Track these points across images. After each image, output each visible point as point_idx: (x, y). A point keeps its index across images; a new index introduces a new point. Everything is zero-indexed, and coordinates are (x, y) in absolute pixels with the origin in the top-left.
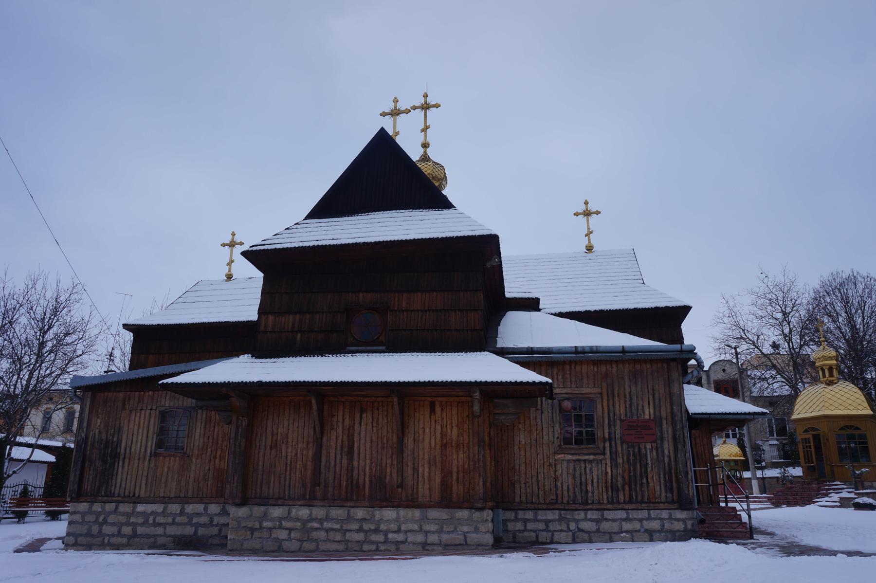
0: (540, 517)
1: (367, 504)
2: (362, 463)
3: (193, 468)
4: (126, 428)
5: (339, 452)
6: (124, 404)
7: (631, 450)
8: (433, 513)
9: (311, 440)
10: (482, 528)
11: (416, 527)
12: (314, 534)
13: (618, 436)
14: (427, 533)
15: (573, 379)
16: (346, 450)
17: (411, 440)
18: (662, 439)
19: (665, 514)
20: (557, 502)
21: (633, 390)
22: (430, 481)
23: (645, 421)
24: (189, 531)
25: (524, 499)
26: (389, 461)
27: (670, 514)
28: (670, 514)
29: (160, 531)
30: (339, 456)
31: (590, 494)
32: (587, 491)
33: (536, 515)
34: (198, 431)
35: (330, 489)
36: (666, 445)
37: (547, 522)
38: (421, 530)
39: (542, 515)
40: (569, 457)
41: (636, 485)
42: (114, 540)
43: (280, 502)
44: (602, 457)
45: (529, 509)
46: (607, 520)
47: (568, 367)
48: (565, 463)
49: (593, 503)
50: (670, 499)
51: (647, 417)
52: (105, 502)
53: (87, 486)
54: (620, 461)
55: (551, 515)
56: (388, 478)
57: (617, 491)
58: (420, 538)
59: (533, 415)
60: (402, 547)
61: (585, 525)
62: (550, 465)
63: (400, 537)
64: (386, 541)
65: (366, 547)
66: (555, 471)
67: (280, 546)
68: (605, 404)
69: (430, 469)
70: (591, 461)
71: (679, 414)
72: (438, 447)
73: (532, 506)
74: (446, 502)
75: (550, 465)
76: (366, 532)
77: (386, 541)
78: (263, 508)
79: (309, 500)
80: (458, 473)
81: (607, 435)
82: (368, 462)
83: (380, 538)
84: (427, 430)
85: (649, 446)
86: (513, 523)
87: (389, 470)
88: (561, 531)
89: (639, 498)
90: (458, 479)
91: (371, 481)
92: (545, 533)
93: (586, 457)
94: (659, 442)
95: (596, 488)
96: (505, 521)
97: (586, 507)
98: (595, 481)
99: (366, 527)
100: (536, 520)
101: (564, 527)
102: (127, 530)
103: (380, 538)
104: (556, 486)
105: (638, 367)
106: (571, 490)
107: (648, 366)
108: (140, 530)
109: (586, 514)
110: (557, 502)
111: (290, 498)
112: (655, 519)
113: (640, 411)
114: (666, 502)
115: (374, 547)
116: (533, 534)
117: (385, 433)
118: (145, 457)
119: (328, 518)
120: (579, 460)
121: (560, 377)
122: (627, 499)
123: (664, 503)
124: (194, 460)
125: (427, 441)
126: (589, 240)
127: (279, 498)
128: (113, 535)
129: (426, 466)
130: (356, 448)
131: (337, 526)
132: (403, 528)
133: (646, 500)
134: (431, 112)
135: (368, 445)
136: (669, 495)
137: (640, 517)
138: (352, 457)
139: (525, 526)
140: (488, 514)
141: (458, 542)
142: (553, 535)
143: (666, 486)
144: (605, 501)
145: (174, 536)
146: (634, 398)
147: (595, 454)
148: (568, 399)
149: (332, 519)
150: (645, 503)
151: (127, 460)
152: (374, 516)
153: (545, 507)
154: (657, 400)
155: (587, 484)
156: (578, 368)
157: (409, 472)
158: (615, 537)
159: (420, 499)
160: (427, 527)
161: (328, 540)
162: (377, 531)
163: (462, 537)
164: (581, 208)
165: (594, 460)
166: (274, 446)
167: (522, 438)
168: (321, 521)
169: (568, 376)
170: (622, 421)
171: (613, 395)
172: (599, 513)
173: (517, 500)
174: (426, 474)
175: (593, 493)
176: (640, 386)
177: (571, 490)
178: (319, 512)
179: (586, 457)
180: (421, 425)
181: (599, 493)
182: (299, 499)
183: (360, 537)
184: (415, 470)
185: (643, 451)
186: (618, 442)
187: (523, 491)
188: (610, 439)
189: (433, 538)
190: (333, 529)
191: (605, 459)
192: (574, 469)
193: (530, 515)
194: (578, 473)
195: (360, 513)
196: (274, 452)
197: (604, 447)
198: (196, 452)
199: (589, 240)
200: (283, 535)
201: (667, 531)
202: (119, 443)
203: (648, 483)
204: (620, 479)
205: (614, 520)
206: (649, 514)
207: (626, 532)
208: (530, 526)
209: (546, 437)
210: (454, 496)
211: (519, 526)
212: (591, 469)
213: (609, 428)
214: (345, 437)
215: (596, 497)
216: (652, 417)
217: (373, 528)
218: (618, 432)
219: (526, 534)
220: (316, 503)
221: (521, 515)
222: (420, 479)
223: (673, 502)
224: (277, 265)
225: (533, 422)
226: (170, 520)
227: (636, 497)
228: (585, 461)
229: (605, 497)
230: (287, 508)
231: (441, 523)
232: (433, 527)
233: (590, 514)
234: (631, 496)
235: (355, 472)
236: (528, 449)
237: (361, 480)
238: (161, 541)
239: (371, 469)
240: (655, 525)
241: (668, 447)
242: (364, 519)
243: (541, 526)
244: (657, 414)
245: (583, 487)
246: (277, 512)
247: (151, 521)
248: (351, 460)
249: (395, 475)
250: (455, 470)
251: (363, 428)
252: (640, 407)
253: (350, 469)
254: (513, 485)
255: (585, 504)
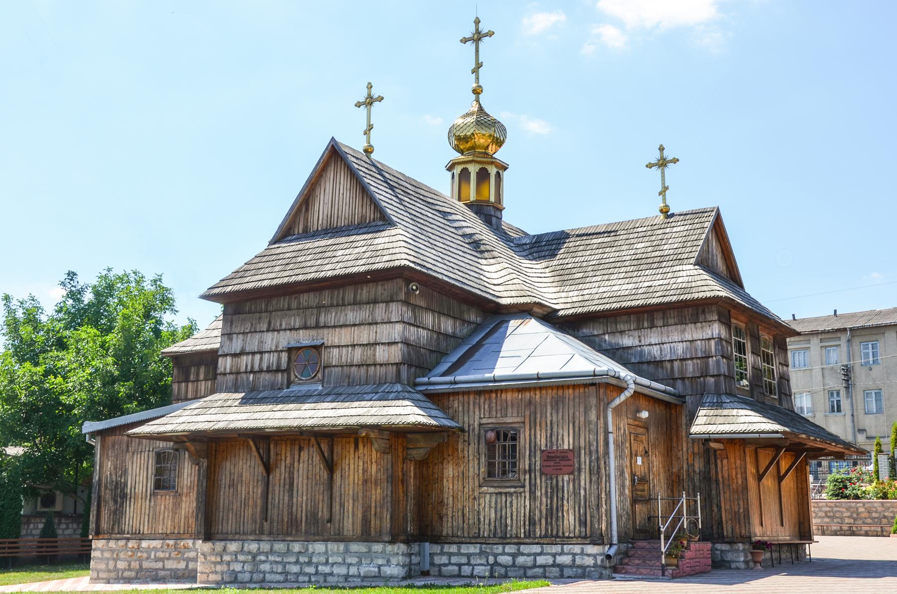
0: (462, 551)
1: (303, 539)
2: (300, 499)
3: (184, 506)
4: (130, 471)
5: (282, 489)
6: (128, 447)
7: (549, 482)
8: (355, 547)
9: (260, 478)
10: (394, 561)
11: (340, 560)
12: (263, 567)
13: (538, 468)
14: (350, 565)
15: (499, 408)
16: (287, 487)
17: (339, 476)
18: (579, 470)
19: (577, 549)
20: (479, 537)
21: (555, 419)
22: (353, 515)
23: (564, 451)
24: (182, 565)
25: (450, 532)
26: (321, 497)
27: (582, 550)
28: (582, 550)
29: (160, 565)
30: (282, 493)
31: (509, 528)
32: (506, 525)
33: (459, 549)
34: (186, 471)
35: (275, 524)
36: (582, 477)
37: (469, 556)
38: (344, 563)
39: (465, 549)
40: (492, 490)
41: (551, 519)
42: (126, 574)
43: (237, 537)
44: (522, 489)
45: (454, 543)
46: (523, 554)
47: (494, 395)
48: (488, 496)
49: (511, 537)
50: (583, 534)
51: (566, 447)
52: (118, 539)
53: (104, 525)
54: (538, 494)
55: (473, 549)
56: (320, 514)
57: (535, 524)
58: (343, 570)
59: (460, 447)
60: (330, 579)
61: (505, 560)
62: (475, 498)
63: (326, 569)
64: (317, 573)
65: (301, 579)
66: (479, 505)
67: (236, 577)
68: (527, 434)
69: (353, 504)
70: (511, 494)
71: (595, 443)
72: (360, 483)
73: (457, 540)
74: (367, 536)
75: (475, 498)
76: (301, 564)
77: (317, 573)
78: (223, 543)
79: (258, 534)
80: (376, 507)
81: (527, 468)
82: (305, 498)
83: (311, 570)
84: (352, 467)
85: (566, 478)
86: (439, 557)
87: (320, 506)
88: (482, 565)
89: (555, 533)
90: (375, 514)
91: (306, 517)
92: (466, 567)
93: (507, 490)
94: (576, 473)
95: (515, 522)
96: (432, 555)
97: (505, 541)
98: (515, 514)
99: (302, 559)
100: (459, 554)
101: (483, 561)
102: (135, 565)
103: (311, 570)
104: (479, 519)
105: (560, 392)
106: (493, 524)
107: (571, 391)
108: (146, 565)
109: (504, 549)
110: (479, 537)
111: (244, 534)
112: (568, 554)
113: (560, 441)
114: (580, 537)
115: (306, 579)
116: (456, 568)
117: (318, 471)
118: (146, 496)
119: (272, 551)
120: (501, 493)
121: (487, 406)
122: (543, 533)
123: (577, 538)
124: (184, 498)
125: (352, 477)
126: (664, 199)
127: (236, 533)
128: (125, 570)
129: (351, 501)
130: (295, 485)
131: (279, 559)
132: (330, 561)
133: (560, 534)
134: (485, 43)
135: (305, 481)
136: (583, 529)
137: (554, 551)
138: (292, 494)
139: (450, 560)
140: (403, 547)
141: (373, 574)
142: (473, 569)
143: (580, 520)
144: (522, 536)
145: (171, 570)
146: (555, 427)
147: (515, 487)
148: (492, 430)
149: (275, 552)
150: (559, 537)
151: (132, 500)
152: (307, 549)
153: (468, 540)
154: (577, 429)
155: (506, 518)
156: (504, 396)
157: (336, 507)
158: (530, 573)
159: (345, 533)
160: (349, 560)
161: (272, 572)
162: (309, 563)
163: (376, 570)
164: (654, 157)
165: (515, 492)
166: (232, 485)
167: (450, 471)
168: (266, 554)
169: (494, 405)
170: (542, 451)
171: (535, 425)
172: (515, 547)
173: (444, 533)
174: (350, 510)
175: (512, 527)
176: (561, 414)
177: (493, 524)
178: (265, 547)
179: (507, 490)
180: (347, 462)
181: (517, 526)
182: (251, 534)
183: (295, 569)
184: (342, 505)
185: (560, 484)
186: (538, 474)
187: (450, 524)
188: (530, 471)
189: (353, 571)
190: (276, 562)
191: (524, 492)
192: (496, 503)
193: (454, 549)
194: (499, 506)
195: (297, 547)
196: (231, 490)
197: (525, 480)
198: (185, 490)
199: (664, 199)
200: (237, 567)
201: (578, 567)
202: (126, 484)
203: (563, 516)
204: (537, 512)
205: (529, 555)
206: (562, 549)
207: (540, 566)
208: (454, 560)
209: (471, 470)
210: (372, 530)
211: (444, 560)
212: (511, 502)
213: (530, 459)
214: (287, 475)
215: (514, 531)
216: (571, 447)
217: (306, 560)
218: (538, 463)
219: (450, 568)
220: (264, 537)
221: (447, 548)
222: (346, 514)
223: (585, 537)
224: (242, 304)
225: (460, 455)
226: (167, 555)
227: (552, 531)
228: (506, 493)
229: (522, 531)
230: (240, 543)
231: (360, 556)
232: (354, 560)
233: (508, 549)
234: (547, 530)
235: (294, 508)
236: (456, 482)
237: (299, 516)
238: (162, 573)
239: (307, 505)
240: (565, 560)
241: (584, 478)
242: (300, 552)
243: (464, 560)
244: (577, 443)
245: (503, 521)
246: (233, 547)
247: (153, 557)
248: (291, 496)
249: (325, 510)
250: (373, 505)
251: (301, 465)
252: (560, 437)
253: (290, 506)
254: (441, 518)
255: (504, 539)
